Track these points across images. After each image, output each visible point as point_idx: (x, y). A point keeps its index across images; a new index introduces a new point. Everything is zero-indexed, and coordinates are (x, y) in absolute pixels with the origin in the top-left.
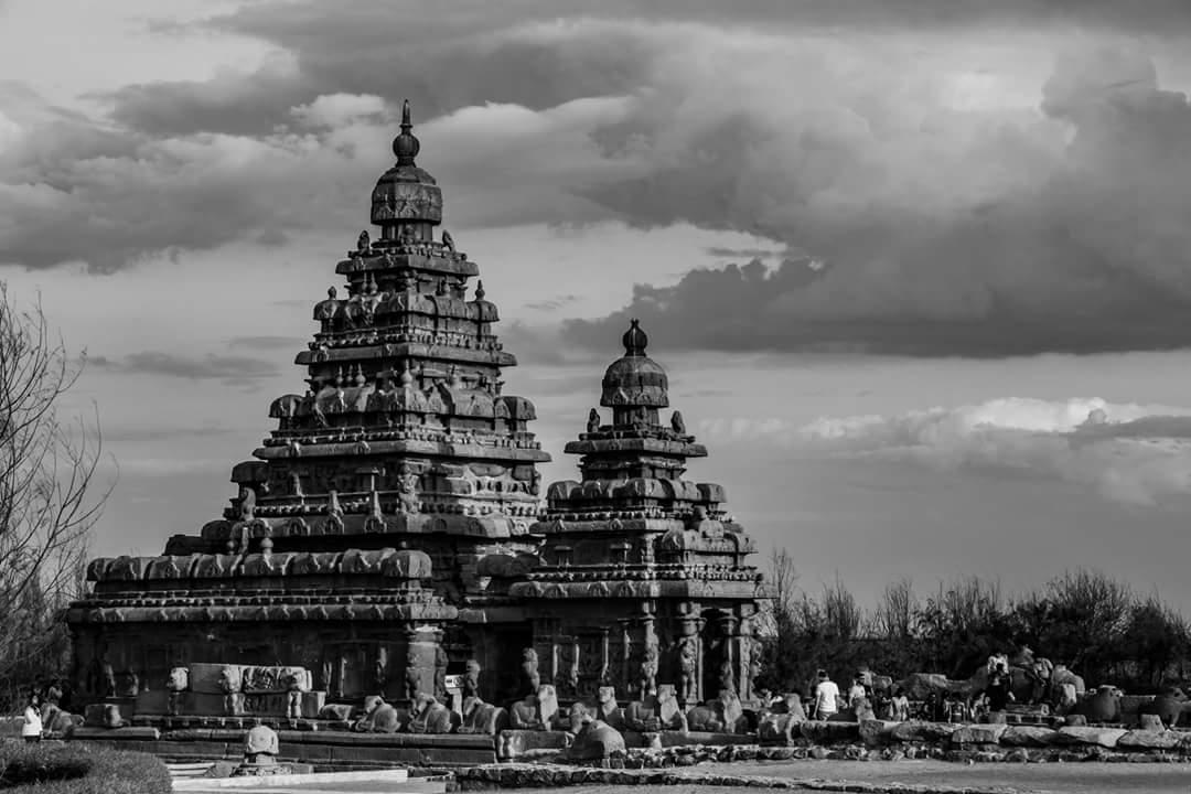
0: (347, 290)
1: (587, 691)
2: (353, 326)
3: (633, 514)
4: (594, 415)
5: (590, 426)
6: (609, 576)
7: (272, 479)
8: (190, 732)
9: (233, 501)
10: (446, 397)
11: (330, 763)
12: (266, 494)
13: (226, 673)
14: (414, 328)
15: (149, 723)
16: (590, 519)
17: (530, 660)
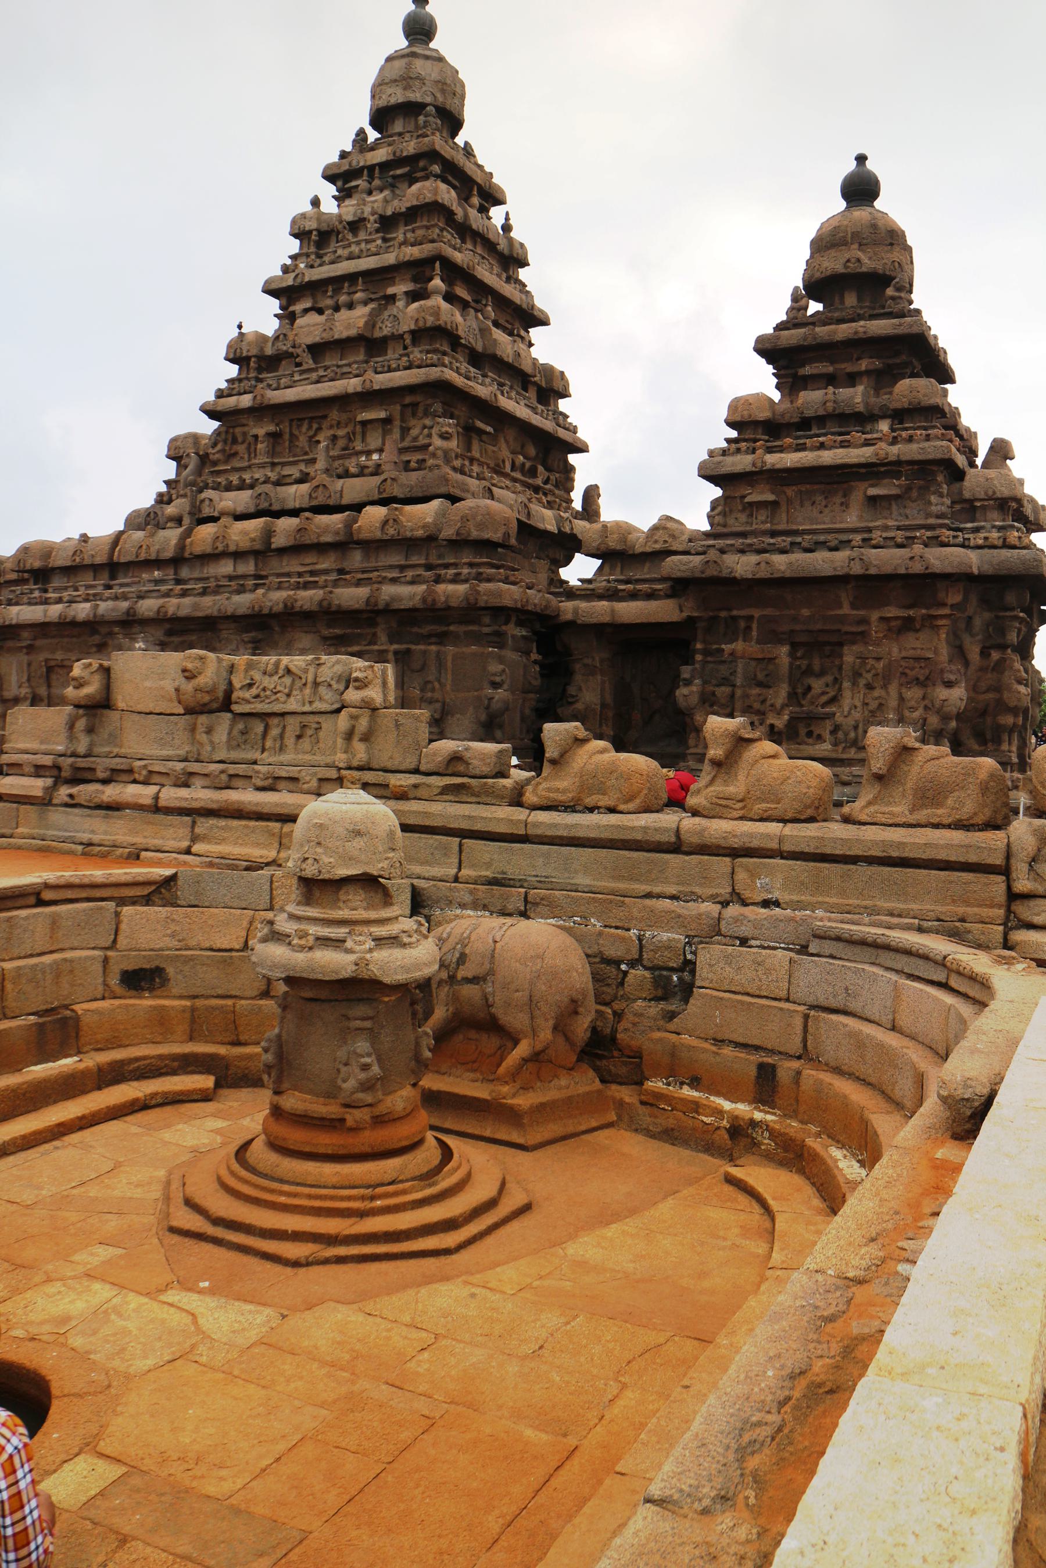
0: (336, 203)
1: (806, 740)
2: (350, 236)
3: (919, 432)
4: (796, 298)
5: (791, 309)
6: (864, 540)
7: (225, 441)
8: (110, 793)
9: (167, 482)
10: (484, 331)
11: (456, 879)
12: (215, 463)
13: (190, 666)
14: (442, 230)
15: (27, 769)
16: (822, 446)
17: (688, 683)
